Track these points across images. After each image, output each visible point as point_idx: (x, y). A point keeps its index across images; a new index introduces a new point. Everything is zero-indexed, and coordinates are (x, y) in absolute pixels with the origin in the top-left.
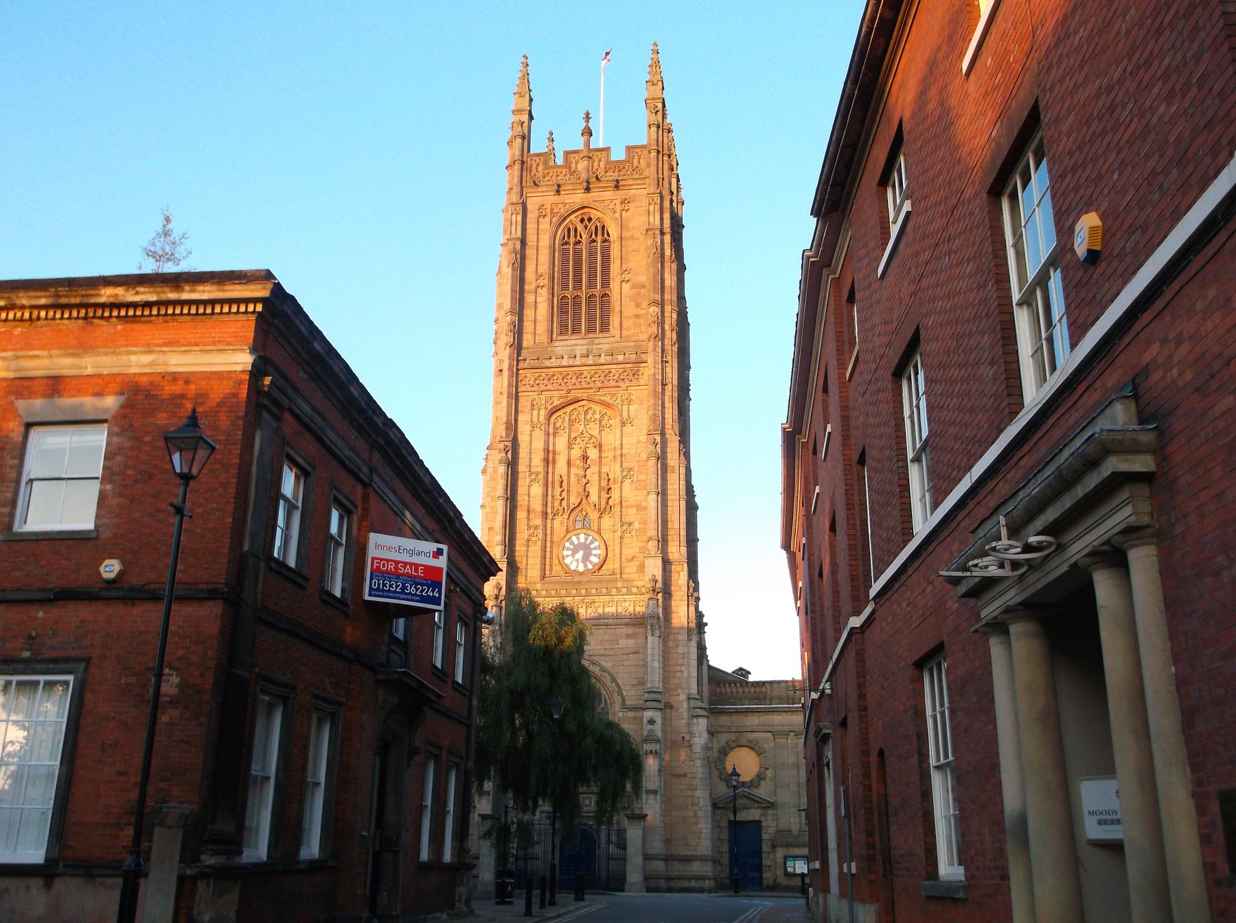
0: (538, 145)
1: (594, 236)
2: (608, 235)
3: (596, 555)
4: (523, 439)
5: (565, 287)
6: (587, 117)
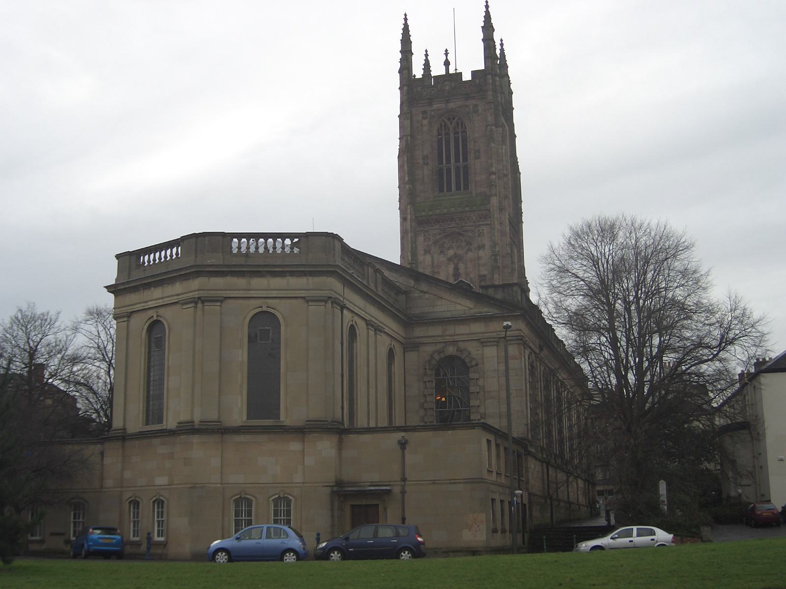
0: (418, 71)
1: (456, 129)
2: (466, 128)
4: (421, 258)
5: (440, 162)
6: (446, 54)
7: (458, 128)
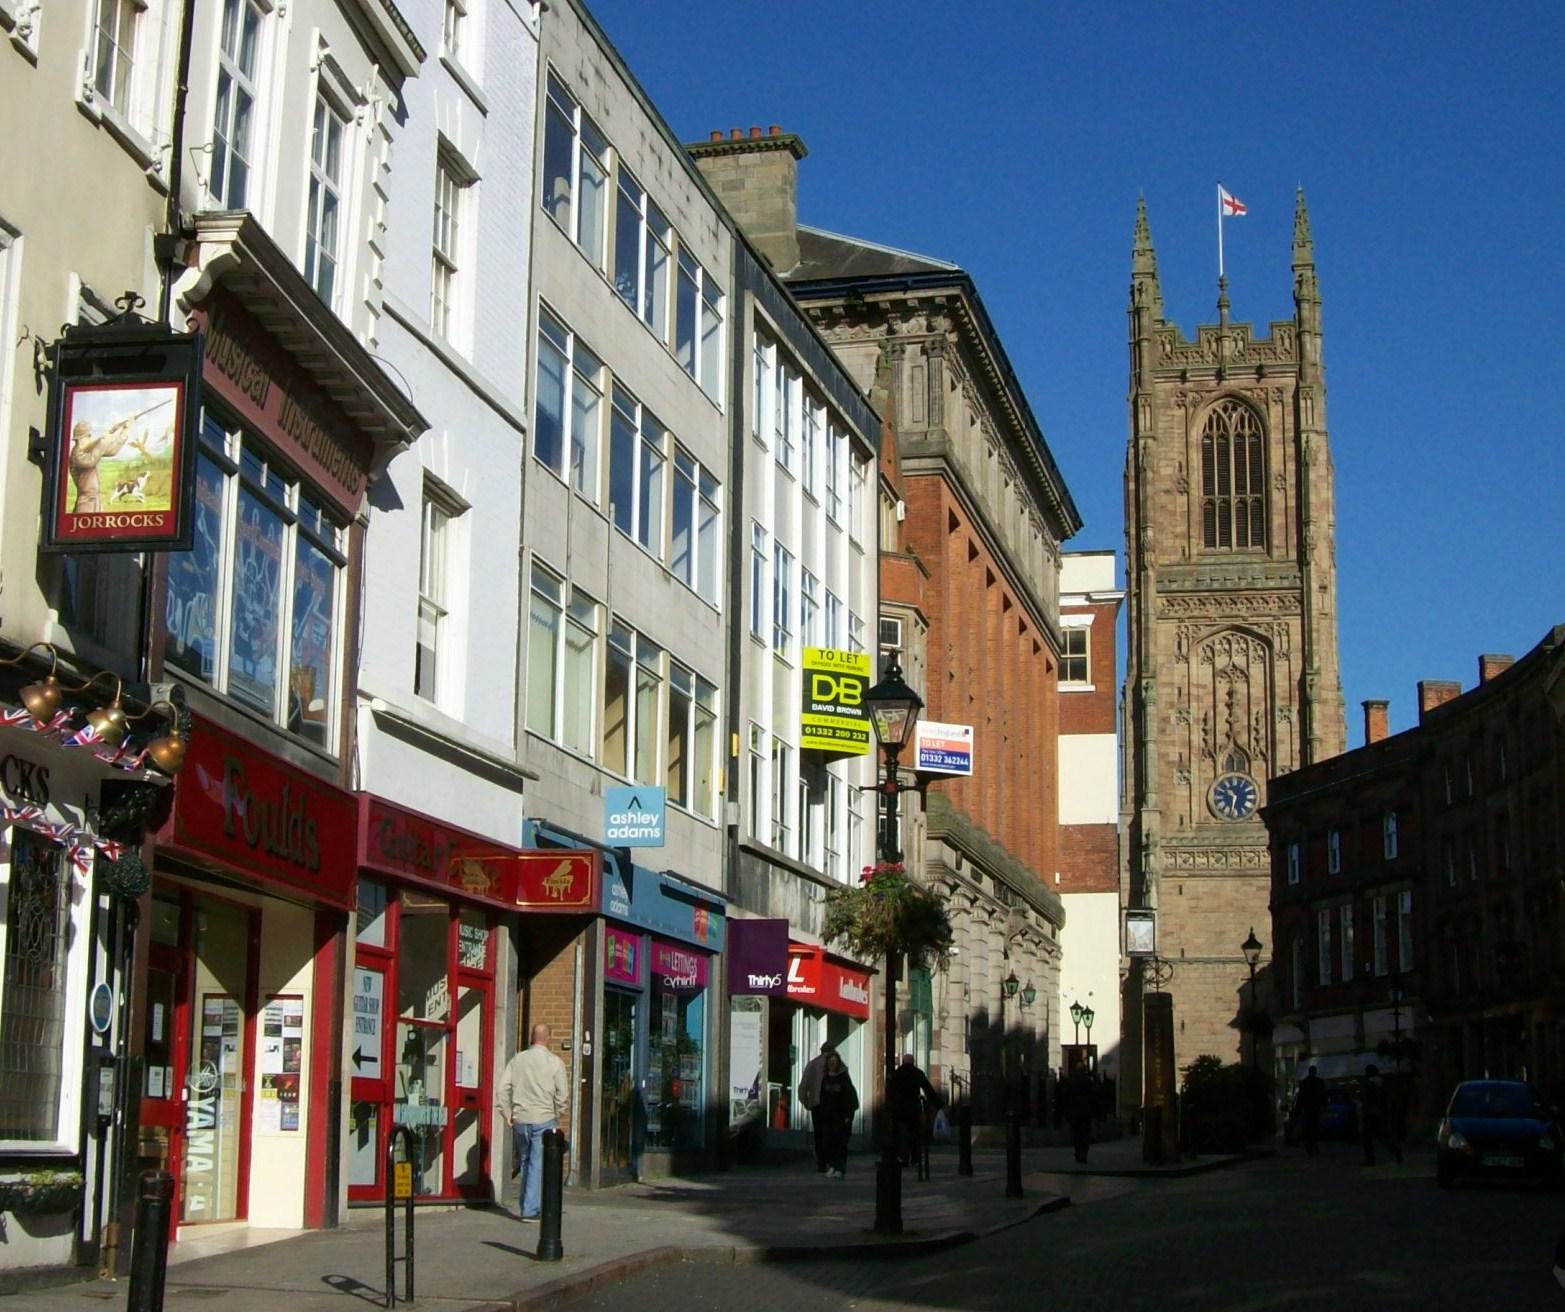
3: (1250, 800)
7: (1243, 427)
